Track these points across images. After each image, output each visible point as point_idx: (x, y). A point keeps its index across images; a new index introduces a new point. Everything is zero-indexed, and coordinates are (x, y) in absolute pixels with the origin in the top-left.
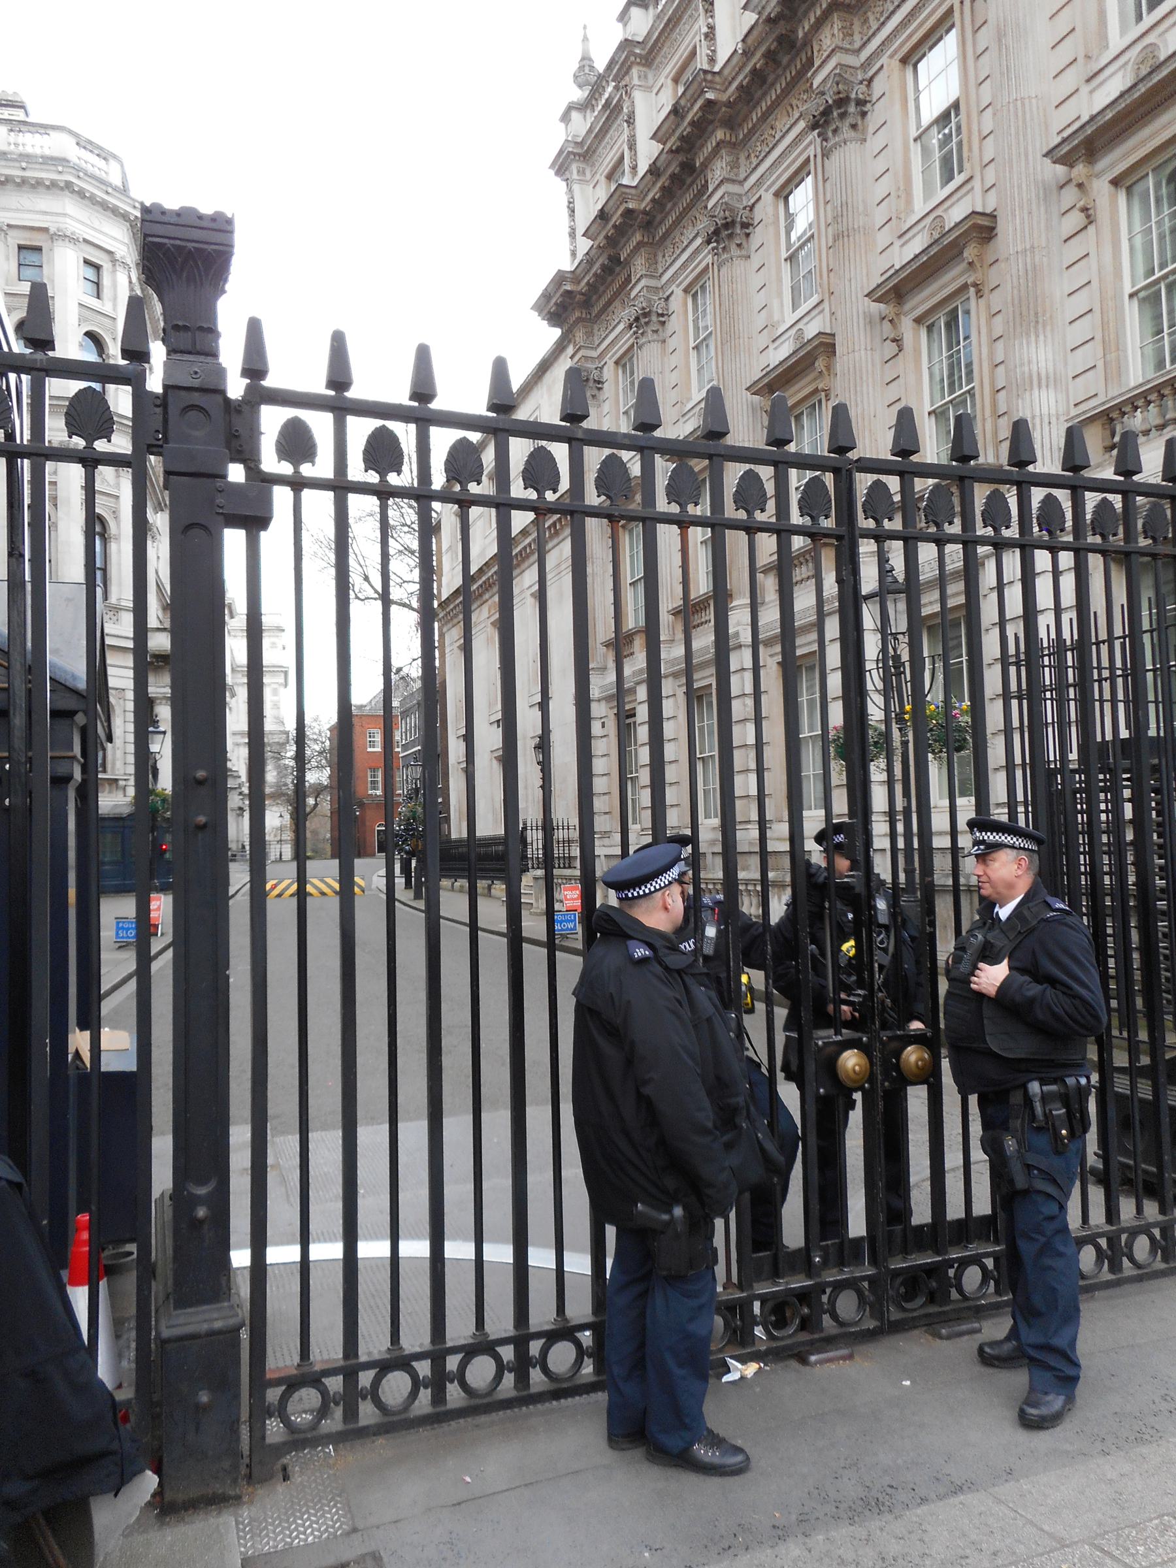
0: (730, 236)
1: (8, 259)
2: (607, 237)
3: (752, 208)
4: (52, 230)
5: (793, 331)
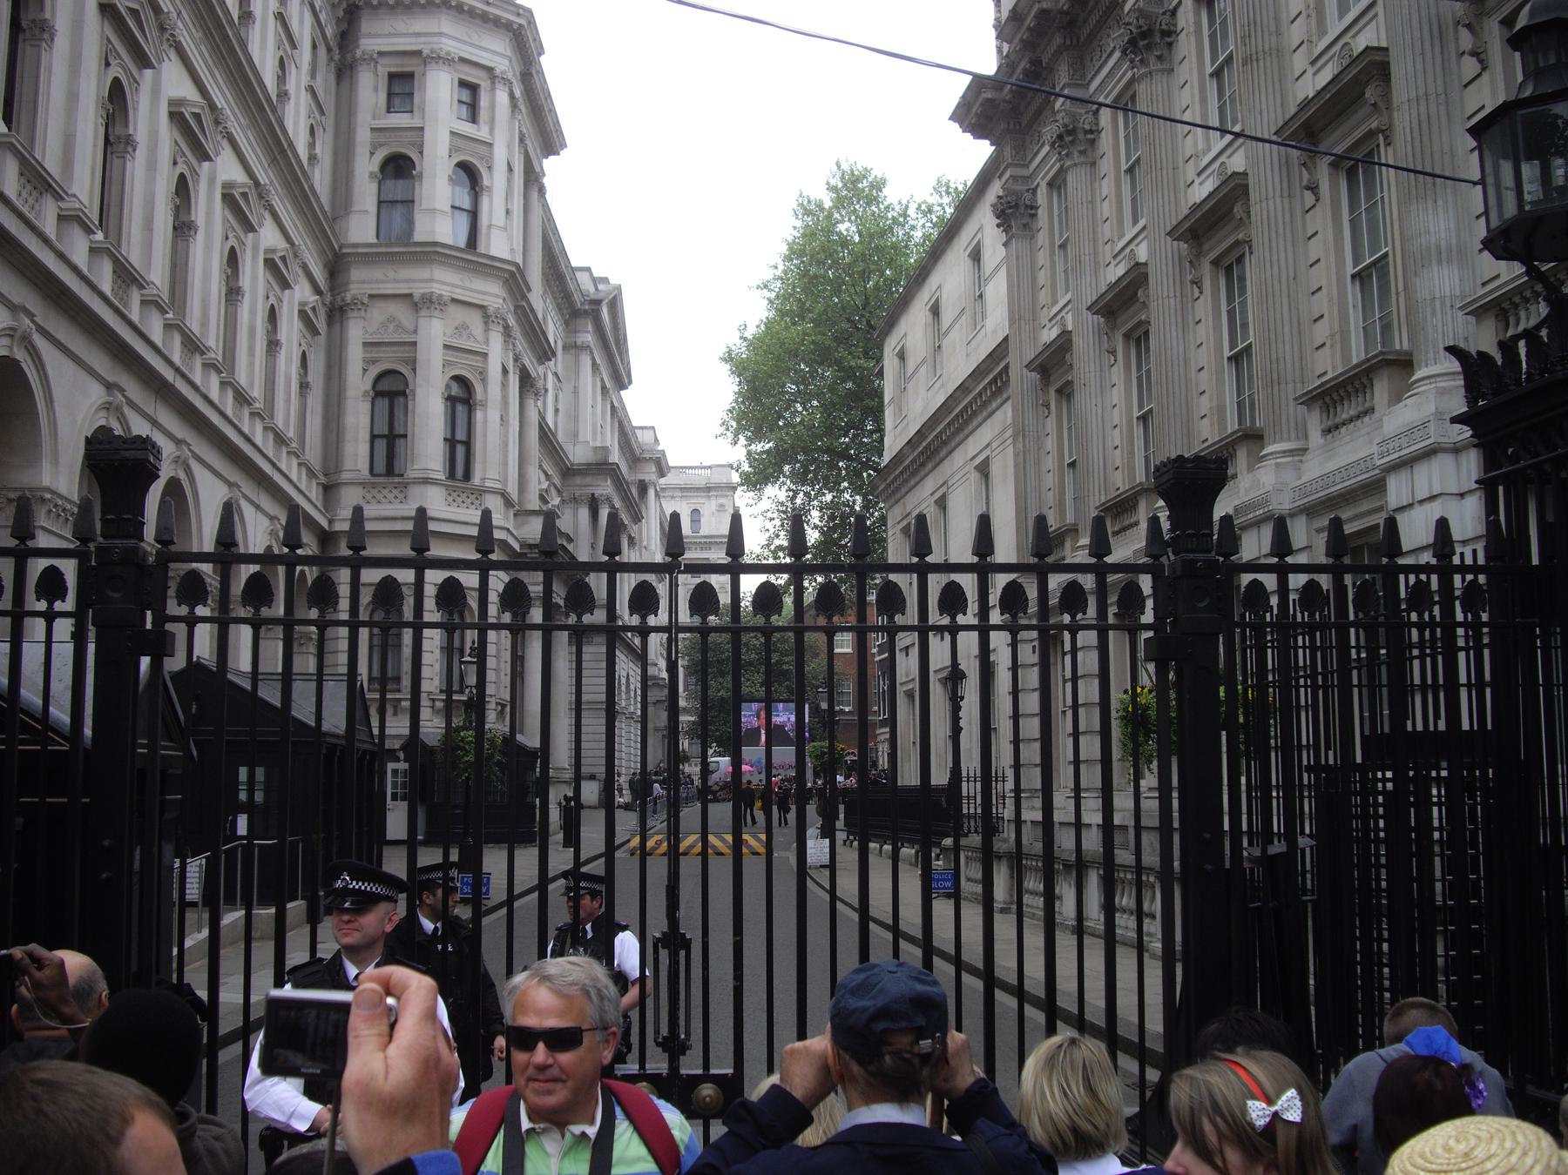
0: (1149, 47)
1: (376, 89)
2: (1022, 40)
3: (1174, 13)
4: (426, 52)
5: (1216, 165)
